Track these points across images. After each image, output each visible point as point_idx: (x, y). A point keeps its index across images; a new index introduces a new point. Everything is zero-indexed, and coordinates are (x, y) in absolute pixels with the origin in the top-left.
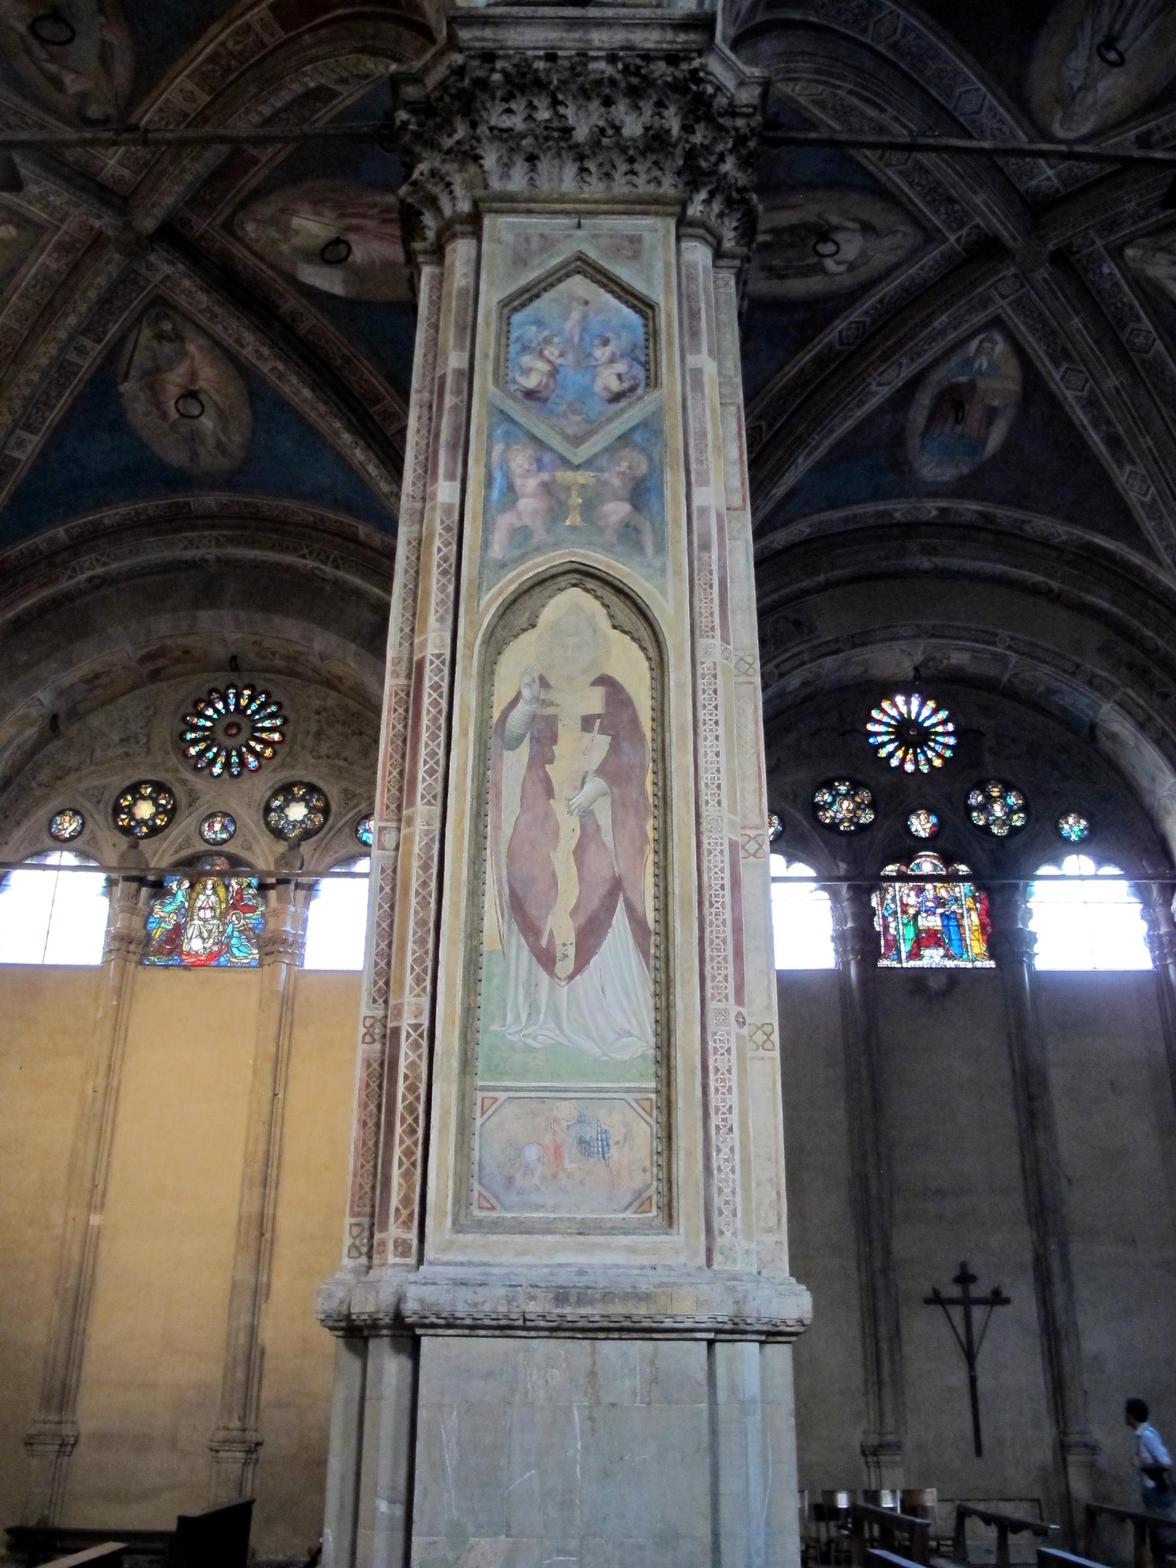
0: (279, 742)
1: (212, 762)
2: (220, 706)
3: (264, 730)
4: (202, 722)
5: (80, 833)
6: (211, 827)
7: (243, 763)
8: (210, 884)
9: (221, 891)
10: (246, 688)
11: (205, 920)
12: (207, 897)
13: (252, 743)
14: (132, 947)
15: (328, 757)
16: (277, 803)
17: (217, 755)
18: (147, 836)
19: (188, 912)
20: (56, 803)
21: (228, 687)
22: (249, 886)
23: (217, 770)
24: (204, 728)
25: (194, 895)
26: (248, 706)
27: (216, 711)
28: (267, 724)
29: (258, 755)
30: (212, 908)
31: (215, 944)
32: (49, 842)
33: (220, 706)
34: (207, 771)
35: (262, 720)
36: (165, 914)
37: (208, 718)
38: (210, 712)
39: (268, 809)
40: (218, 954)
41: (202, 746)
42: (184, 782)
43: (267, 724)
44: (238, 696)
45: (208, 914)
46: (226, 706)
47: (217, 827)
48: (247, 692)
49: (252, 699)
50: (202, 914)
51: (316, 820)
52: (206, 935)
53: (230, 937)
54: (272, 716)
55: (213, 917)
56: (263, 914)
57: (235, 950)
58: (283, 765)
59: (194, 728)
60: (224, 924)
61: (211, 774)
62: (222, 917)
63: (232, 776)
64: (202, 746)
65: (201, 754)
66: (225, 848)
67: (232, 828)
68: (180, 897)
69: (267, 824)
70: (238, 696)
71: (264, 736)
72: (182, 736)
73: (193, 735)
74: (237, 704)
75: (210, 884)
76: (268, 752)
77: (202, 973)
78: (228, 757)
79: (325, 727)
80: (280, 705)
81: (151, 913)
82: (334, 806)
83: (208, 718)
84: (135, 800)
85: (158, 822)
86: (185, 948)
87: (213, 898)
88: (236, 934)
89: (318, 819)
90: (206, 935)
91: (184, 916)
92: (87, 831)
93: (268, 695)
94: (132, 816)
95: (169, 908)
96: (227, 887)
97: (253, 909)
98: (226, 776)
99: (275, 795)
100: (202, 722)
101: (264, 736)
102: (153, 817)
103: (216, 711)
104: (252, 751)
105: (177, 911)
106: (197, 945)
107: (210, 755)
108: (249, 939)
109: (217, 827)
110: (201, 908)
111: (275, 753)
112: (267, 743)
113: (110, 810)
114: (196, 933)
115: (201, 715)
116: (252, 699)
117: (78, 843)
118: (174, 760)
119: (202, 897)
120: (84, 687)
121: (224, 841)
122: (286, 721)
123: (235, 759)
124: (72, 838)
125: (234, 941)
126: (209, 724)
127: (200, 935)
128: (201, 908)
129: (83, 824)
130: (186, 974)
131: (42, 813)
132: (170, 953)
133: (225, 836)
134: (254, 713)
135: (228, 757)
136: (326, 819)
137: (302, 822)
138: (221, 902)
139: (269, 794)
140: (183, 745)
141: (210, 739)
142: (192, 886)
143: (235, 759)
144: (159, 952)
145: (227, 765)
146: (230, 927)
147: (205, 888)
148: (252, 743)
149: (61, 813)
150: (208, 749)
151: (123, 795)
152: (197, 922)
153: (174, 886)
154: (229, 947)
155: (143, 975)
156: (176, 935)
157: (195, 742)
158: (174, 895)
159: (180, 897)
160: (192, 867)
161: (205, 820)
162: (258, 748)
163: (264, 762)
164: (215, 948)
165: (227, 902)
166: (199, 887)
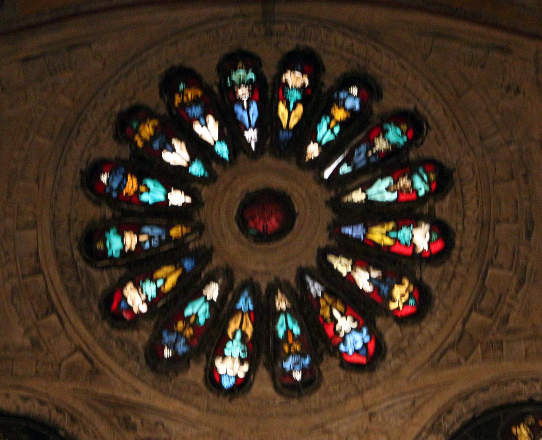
0: (431, 258)
1: (211, 339)
2: (209, 131)
3: (374, 213)
4: (154, 193)
7: (319, 340)
10: (290, 62)
13: (342, 266)
17: (222, 311)
21: (228, 64)
23: (231, 366)
24: (162, 212)
26: (306, 130)
27: (199, 149)
28: (382, 191)
29: (367, 309)
33: (209, 131)
34: (195, 373)
35: (365, 177)
37: (175, 177)
38: (177, 156)
41: (168, 278)
43: (382, 191)
44: (268, 93)
46: (231, 131)
48: (295, 79)
49: (317, 103)
54: (393, 164)
58: (464, 344)
59: (134, 215)
61: (213, 378)
63: (285, 385)
64: (168, 278)
65: (168, 308)
70: (268, 93)
71: (378, 235)
74: (268, 122)
76: (400, 295)
78: (264, 316)
80: (413, 123)
83: (175, 177)
93: (371, 90)
98: (263, 386)
100: (154, 193)
101: (378, 235)
103: (199, 149)
104: (343, 291)
107: (198, 310)
111: (422, 295)
112: (393, 264)
116: (317, 103)
118: (81, 330)
122: (444, 180)
123: (287, 326)
135: (264, 316)
140: (103, 280)
141: (185, 250)
143: (287, 326)
145: (263, 349)
148: (342, 266)
150: (189, 289)
157: (138, 267)
163: (391, 333)
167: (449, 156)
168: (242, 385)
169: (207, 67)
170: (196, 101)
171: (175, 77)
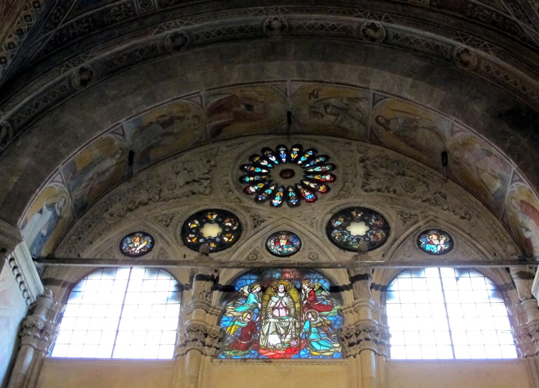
0: (330, 181)
1: (272, 196)
4: (258, 170)
5: (150, 250)
6: (277, 242)
8: (281, 288)
9: (294, 293)
10: (295, 146)
11: (280, 319)
12: (280, 300)
13: (307, 183)
14: (208, 340)
15: (379, 190)
16: (338, 223)
18: (215, 250)
19: (263, 312)
20: (126, 227)
22: (321, 288)
23: (277, 201)
24: (260, 174)
25: (267, 297)
27: (270, 162)
28: (318, 169)
30: (286, 308)
31: (292, 339)
32: (119, 256)
36: (237, 316)
38: (265, 163)
39: (330, 228)
40: (298, 349)
41: (261, 186)
42: (247, 209)
43: (318, 169)
44: (288, 153)
45: (283, 313)
46: (279, 159)
47: (283, 242)
48: (296, 150)
49: (301, 154)
50: (276, 312)
51: (379, 235)
52: (282, 331)
53: (310, 332)
54: (320, 164)
55: (289, 316)
56: (340, 311)
57: (315, 344)
58: (338, 197)
60: (300, 322)
61: (272, 205)
62: (298, 316)
64: (261, 186)
65: (260, 192)
66: (293, 259)
67: (297, 243)
68: (252, 299)
69: (332, 240)
70: (288, 153)
71: (317, 177)
72: (242, 180)
73: (252, 179)
74: (288, 158)
75: (281, 288)
77: (284, 366)
79: (372, 170)
81: (224, 312)
82: (392, 225)
84: (202, 225)
85: (226, 239)
86: (262, 343)
87: (285, 299)
88: (314, 329)
89: (380, 234)
90: (282, 331)
91: (258, 315)
92: (156, 248)
93: (315, 151)
94: (199, 235)
95: (242, 309)
96: (299, 290)
97: (329, 308)
99: (335, 217)
100: (258, 170)
101: (317, 177)
102: (220, 236)
103: (270, 162)
105: (250, 311)
106: (274, 340)
108: (329, 335)
109: (283, 242)
110: (274, 308)
112: (320, 183)
113: (179, 232)
114: (272, 329)
115: (257, 165)
116: (301, 154)
117: (148, 257)
119: (275, 299)
120: (160, 130)
121: (289, 254)
124: (142, 254)
125: (313, 336)
126: (264, 171)
127: (277, 331)
128: (274, 308)
129: (153, 243)
130: (267, 366)
131: (114, 235)
132: (246, 348)
133: (291, 249)
134: (304, 163)
135: (286, 192)
136: (388, 235)
137: (365, 236)
138: (295, 303)
139: (329, 216)
140: (244, 186)
142: (263, 290)
144: (235, 346)
146: (307, 323)
147: (277, 291)
148: (307, 183)
149: (132, 235)
150: (267, 187)
151: (191, 219)
152: (272, 320)
153: (246, 290)
154: (308, 342)
155: (218, 369)
156: (251, 333)
157: (253, 183)
158: (246, 298)
159: (252, 299)
160: (262, 275)
161: (270, 238)
162: (312, 186)
164: (294, 343)
165: (301, 303)
166: (270, 291)
167: (336, 162)
168: (279, 206)
169: (274, 148)
170: (270, 154)
171: (264, 150)
